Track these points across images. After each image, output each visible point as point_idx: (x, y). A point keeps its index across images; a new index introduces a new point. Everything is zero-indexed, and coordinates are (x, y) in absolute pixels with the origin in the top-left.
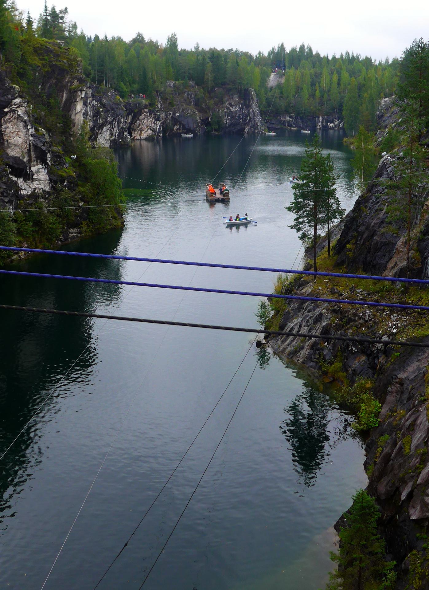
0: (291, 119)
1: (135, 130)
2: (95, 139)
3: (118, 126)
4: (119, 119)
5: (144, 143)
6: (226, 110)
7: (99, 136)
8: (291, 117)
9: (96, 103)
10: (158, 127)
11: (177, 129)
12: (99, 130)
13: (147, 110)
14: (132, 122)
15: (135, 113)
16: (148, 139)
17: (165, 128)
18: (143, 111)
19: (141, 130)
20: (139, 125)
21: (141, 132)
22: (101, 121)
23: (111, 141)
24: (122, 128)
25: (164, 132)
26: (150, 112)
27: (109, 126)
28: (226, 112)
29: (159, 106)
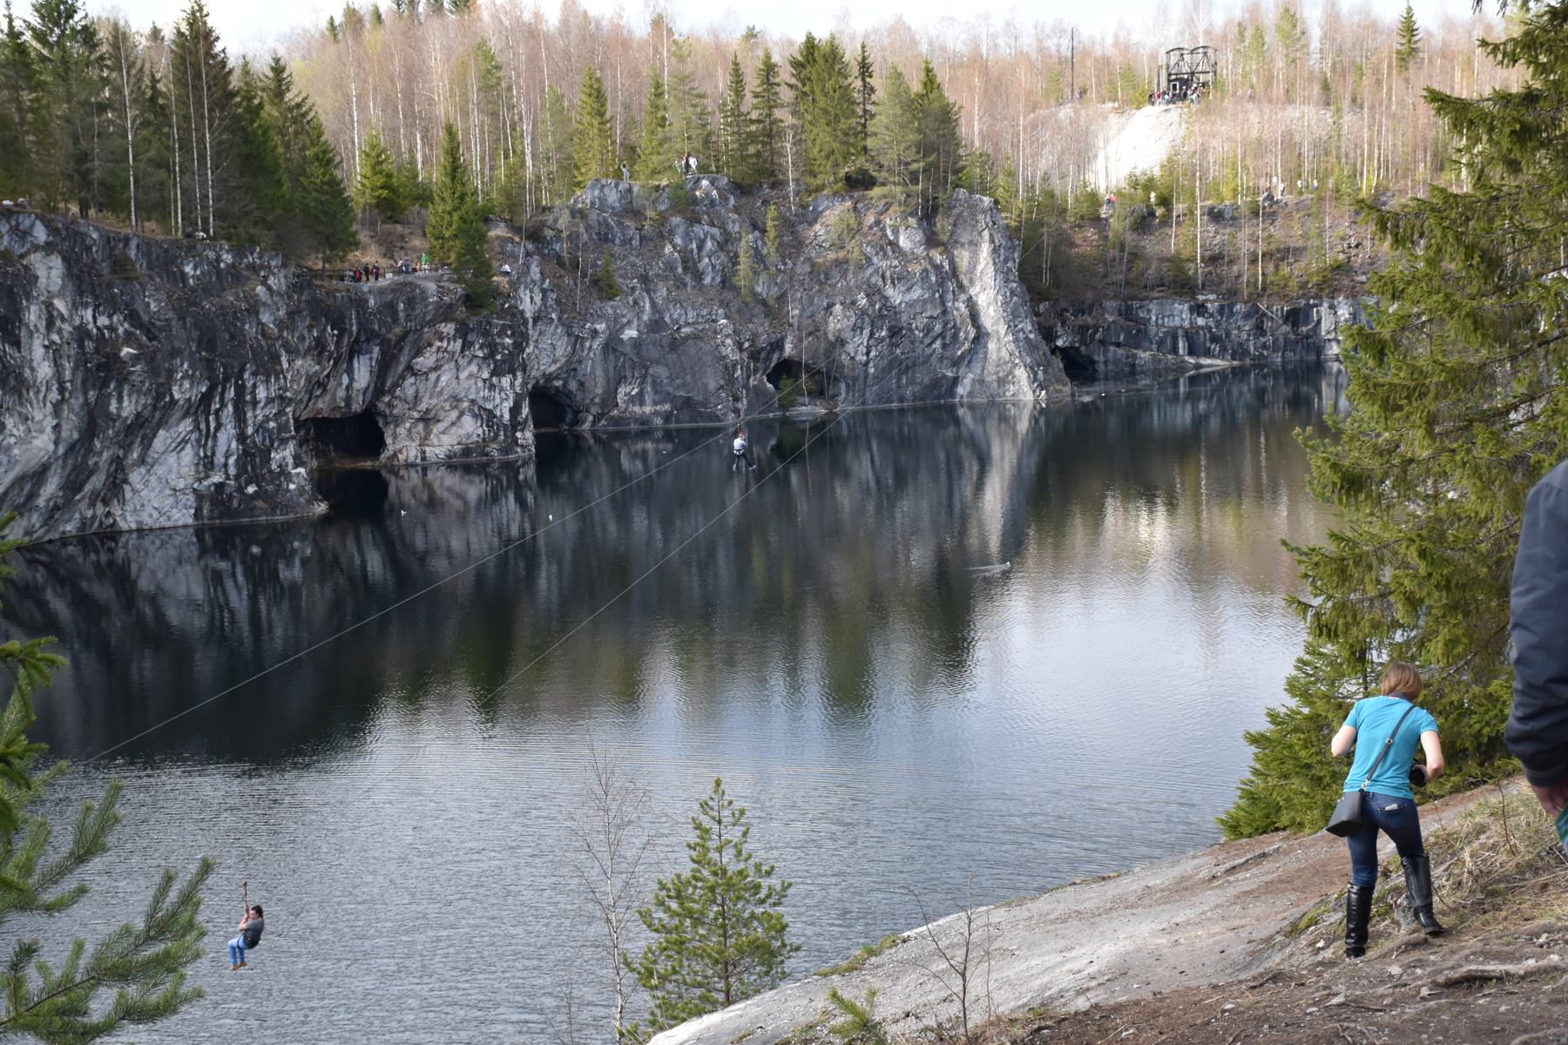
0: (1200, 321)
1: (398, 421)
2: (115, 486)
3: (240, 419)
4: (240, 391)
5: (445, 482)
7: (135, 477)
8: (1199, 309)
9: (103, 321)
10: (509, 404)
11: (632, 400)
12: (127, 448)
13: (448, 328)
14: (379, 387)
15: (392, 337)
16: (466, 462)
17: (550, 403)
19: (428, 420)
20: (417, 398)
21: (428, 433)
22: (127, 407)
23: (199, 496)
24: (260, 428)
26: (463, 331)
27: (186, 426)
28: (863, 312)
29: (528, 303)
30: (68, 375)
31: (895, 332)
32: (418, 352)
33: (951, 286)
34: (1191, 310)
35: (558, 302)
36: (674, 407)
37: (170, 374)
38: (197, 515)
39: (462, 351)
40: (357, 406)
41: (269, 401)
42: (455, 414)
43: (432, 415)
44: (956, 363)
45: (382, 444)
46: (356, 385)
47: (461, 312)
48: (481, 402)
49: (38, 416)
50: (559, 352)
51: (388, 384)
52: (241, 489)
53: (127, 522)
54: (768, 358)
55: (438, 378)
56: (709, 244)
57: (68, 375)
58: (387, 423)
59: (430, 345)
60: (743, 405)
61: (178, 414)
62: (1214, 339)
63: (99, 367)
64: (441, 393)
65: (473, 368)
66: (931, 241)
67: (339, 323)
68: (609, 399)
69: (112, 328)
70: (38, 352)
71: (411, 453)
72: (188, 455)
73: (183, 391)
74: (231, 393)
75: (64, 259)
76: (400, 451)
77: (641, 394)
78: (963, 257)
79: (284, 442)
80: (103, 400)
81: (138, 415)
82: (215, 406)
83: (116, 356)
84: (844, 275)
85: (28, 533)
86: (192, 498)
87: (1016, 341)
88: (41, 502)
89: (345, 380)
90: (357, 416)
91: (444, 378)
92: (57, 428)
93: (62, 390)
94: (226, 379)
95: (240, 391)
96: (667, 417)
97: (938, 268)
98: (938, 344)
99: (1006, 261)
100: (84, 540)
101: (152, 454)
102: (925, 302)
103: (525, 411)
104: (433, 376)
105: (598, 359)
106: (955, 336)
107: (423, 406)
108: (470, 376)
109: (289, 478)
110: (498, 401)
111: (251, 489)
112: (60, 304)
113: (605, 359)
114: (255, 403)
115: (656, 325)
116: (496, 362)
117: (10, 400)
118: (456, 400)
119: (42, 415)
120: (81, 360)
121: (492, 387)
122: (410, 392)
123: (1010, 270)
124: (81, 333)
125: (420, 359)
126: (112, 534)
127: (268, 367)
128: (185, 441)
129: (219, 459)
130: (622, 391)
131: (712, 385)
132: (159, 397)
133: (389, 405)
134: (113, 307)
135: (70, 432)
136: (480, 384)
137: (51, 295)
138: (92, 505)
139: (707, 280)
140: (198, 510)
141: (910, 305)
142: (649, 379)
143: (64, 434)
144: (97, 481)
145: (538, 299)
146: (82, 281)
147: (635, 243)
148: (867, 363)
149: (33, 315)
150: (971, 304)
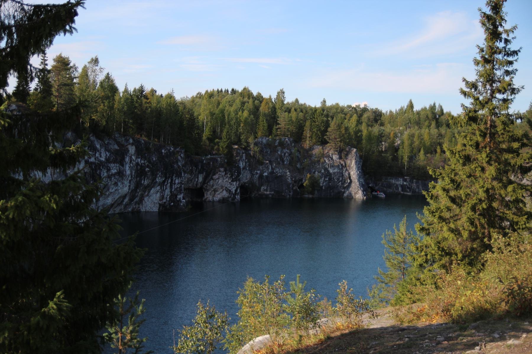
0: (405, 183)
1: (208, 190)
2: (141, 201)
3: (171, 187)
4: (172, 180)
6: (323, 171)
7: (146, 199)
9: (143, 162)
12: (145, 192)
13: (222, 169)
16: (223, 201)
17: (244, 189)
19: (215, 191)
20: (213, 186)
22: (146, 182)
23: (160, 205)
24: (176, 189)
25: (242, 194)
26: (225, 170)
27: (158, 188)
28: (323, 174)
29: (242, 165)
30: (133, 174)
31: (330, 179)
32: (214, 174)
33: (344, 169)
34: (403, 180)
35: (249, 165)
37: (157, 175)
38: (159, 209)
40: (199, 186)
41: (178, 183)
42: (221, 190)
44: (344, 188)
45: (204, 196)
47: (226, 166)
49: (126, 183)
50: (248, 177)
52: (170, 204)
53: (143, 210)
54: (299, 183)
56: (287, 154)
57: (133, 174)
60: (291, 194)
61: (157, 185)
62: (408, 188)
63: (140, 172)
65: (227, 179)
66: (340, 158)
67: (196, 166)
68: (259, 189)
69: (144, 164)
70: (127, 168)
71: (210, 198)
72: (158, 195)
73: (159, 180)
74: (170, 181)
75: (136, 147)
78: (348, 162)
79: (181, 193)
80: (141, 180)
81: (148, 184)
82: (166, 184)
83: (144, 170)
84: (319, 165)
85: (121, 210)
86: (158, 205)
87: (360, 184)
88: (124, 203)
89: (196, 180)
92: (130, 186)
93: (132, 177)
94: (169, 177)
95: (172, 180)
96: (273, 195)
97: (342, 165)
100: (133, 212)
101: (150, 194)
102: (338, 173)
103: (238, 191)
104: (217, 181)
106: (345, 182)
107: (214, 188)
108: (226, 181)
109: (181, 202)
111: (172, 204)
112: (133, 157)
114: (175, 184)
115: (272, 173)
117: (120, 179)
118: (222, 187)
119: (127, 183)
120: (137, 170)
121: (231, 184)
122: (211, 184)
124: (137, 164)
126: (139, 212)
127: (179, 176)
128: (158, 191)
129: (165, 196)
130: (262, 188)
131: (284, 189)
132: (153, 180)
133: (206, 186)
134: (145, 159)
135: (132, 187)
137: (132, 155)
138: (135, 204)
139: (285, 163)
140: (159, 208)
141: (334, 173)
143: (131, 187)
144: (137, 199)
145: (244, 164)
146: (139, 153)
147: (269, 152)
149: (127, 159)
150: (349, 174)
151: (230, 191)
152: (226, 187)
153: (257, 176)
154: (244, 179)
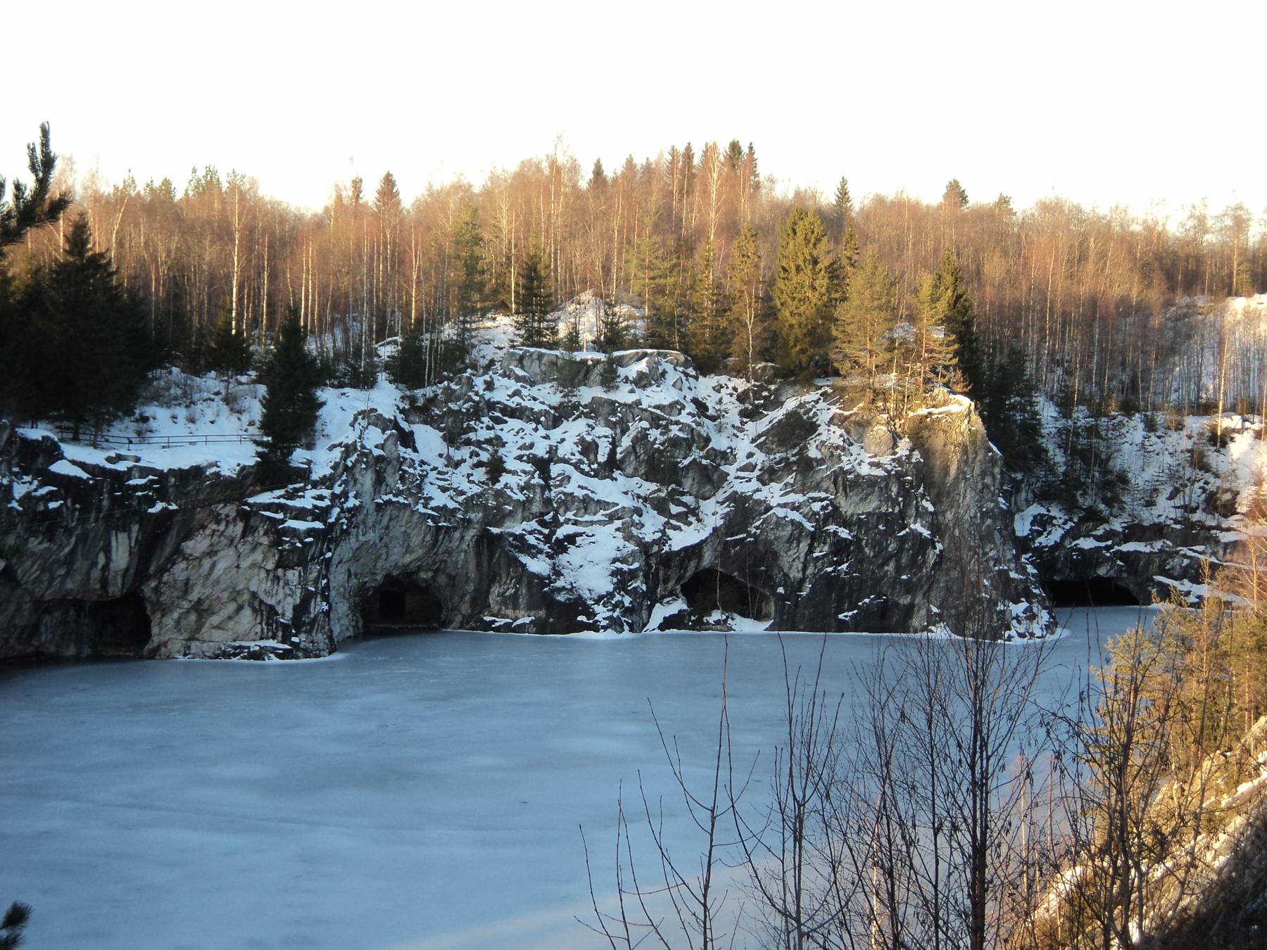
1: (165, 610)
18: (200, 514)
19: (201, 610)
20: (187, 586)
32: (188, 535)
36: (548, 615)
39: (244, 535)
40: (115, 589)
42: (232, 607)
43: (205, 606)
45: (148, 635)
46: (112, 566)
48: (262, 596)
50: (415, 541)
51: (152, 568)
54: (683, 566)
55: (214, 565)
58: (154, 612)
59: (204, 527)
64: (217, 582)
65: (258, 556)
76: (165, 644)
77: (515, 597)
90: (114, 602)
91: (221, 566)
98: (890, 567)
99: (983, 474)
104: (207, 563)
105: (472, 554)
107: (194, 596)
108: (253, 566)
110: (281, 596)
113: (478, 554)
116: (281, 552)
123: (985, 486)
125: (190, 543)
130: (495, 590)
136: (263, 574)
142: (525, 581)
148: (802, 581)
151: (272, 611)
152: (254, 595)
153: (471, 534)
154: (397, 550)
